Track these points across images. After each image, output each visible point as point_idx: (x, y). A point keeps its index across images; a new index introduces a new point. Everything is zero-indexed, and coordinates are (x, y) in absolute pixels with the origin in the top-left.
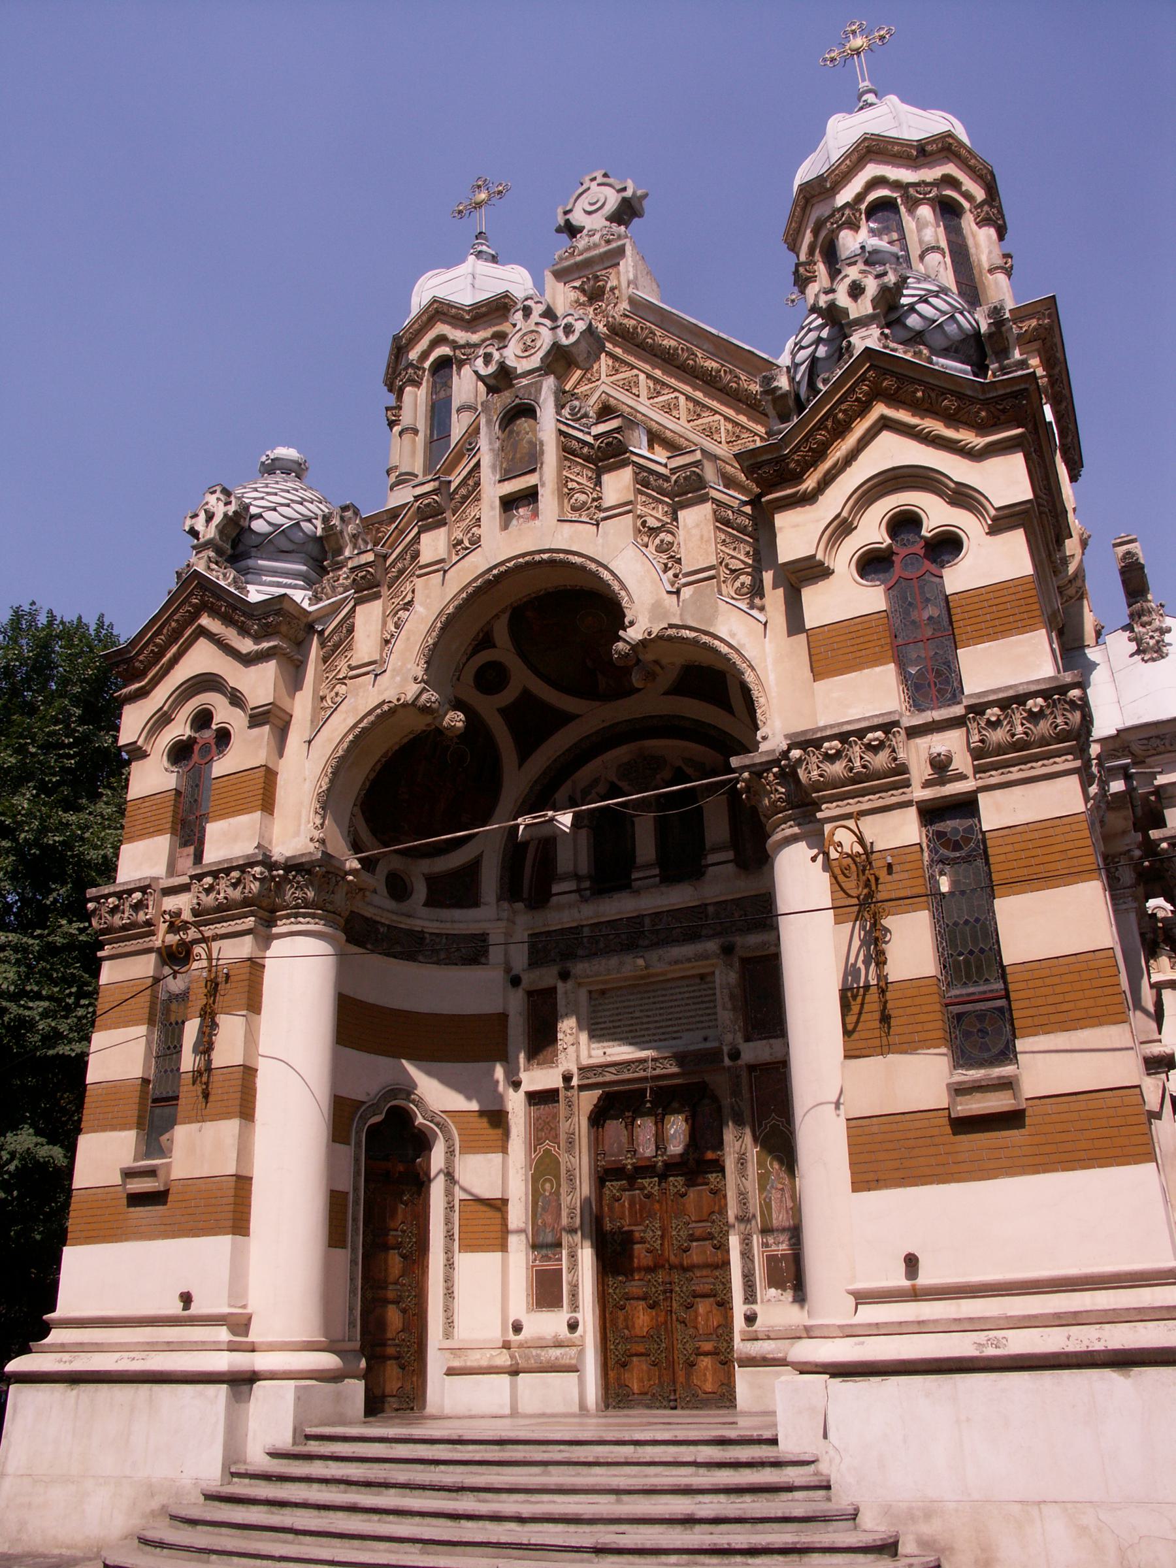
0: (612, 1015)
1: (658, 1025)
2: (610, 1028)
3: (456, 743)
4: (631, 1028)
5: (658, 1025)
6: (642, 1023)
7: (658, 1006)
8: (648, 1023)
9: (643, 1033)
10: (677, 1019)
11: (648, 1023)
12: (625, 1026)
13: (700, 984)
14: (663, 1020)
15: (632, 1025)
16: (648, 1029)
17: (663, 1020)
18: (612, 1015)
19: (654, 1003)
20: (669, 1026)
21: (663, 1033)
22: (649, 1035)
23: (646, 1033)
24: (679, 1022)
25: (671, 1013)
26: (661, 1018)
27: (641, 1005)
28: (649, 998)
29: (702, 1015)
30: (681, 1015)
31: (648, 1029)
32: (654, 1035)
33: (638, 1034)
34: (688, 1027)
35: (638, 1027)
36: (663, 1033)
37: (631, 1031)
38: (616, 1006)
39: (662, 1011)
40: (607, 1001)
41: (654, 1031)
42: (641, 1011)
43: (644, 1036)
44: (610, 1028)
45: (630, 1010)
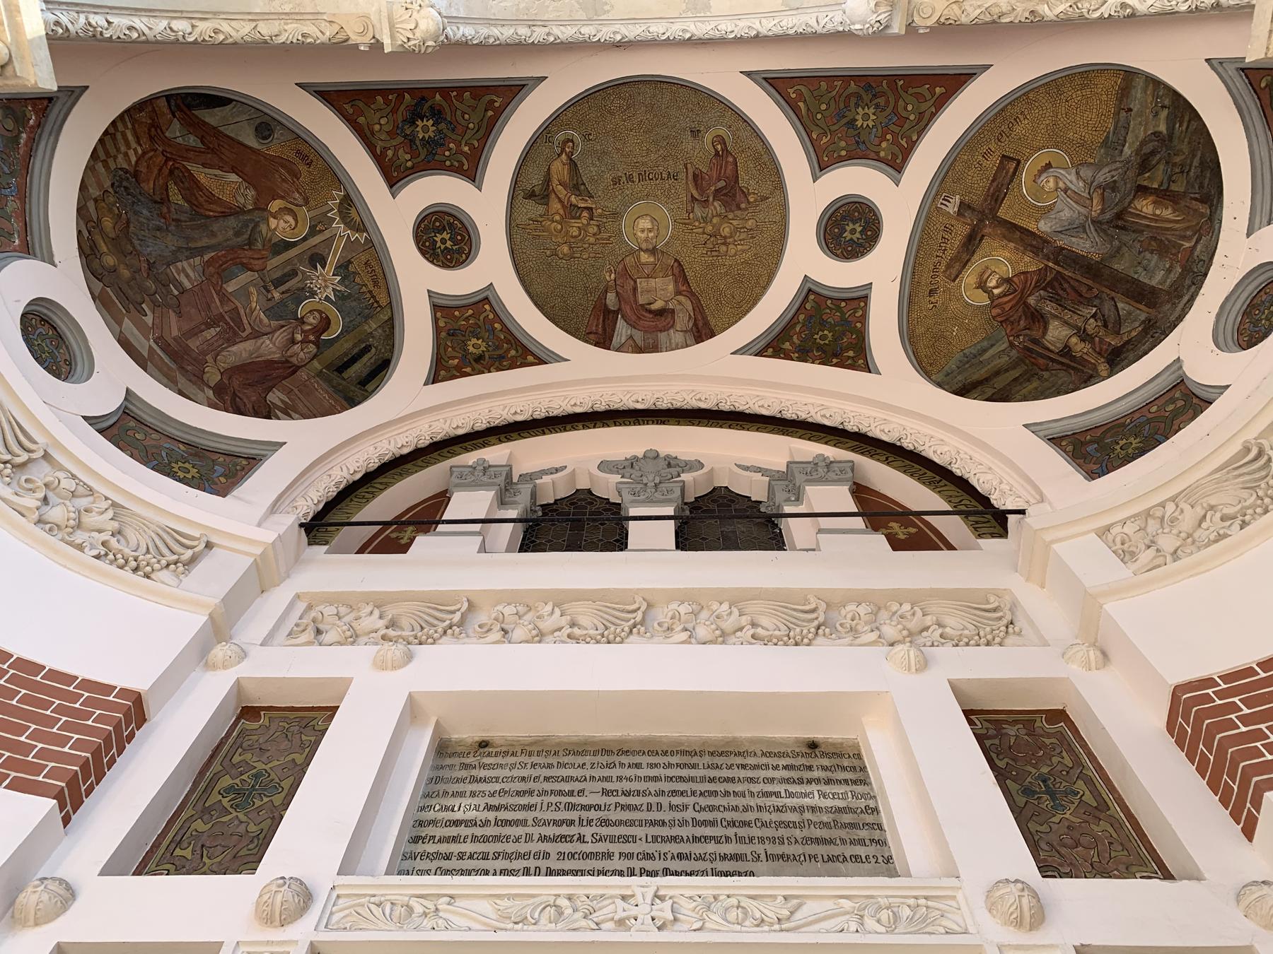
0: (503, 792)
1: (665, 831)
2: (486, 823)
3: (327, 298)
4: (564, 830)
5: (665, 831)
6: (605, 823)
7: (667, 787)
8: (631, 823)
9: (601, 847)
10: (732, 824)
11: (631, 823)
12: (537, 822)
13: (809, 755)
14: (683, 823)
15: (572, 823)
16: (626, 839)
17: (683, 823)
18: (503, 792)
19: (656, 779)
20: (706, 839)
21: (681, 856)
22: (629, 856)
23: (615, 848)
24: (742, 832)
25: (712, 808)
26: (678, 815)
27: (607, 779)
28: (638, 766)
29: (826, 825)
30: (750, 816)
31: (626, 839)
32: (649, 856)
33: (588, 848)
34: (778, 849)
35: (587, 831)
36: (681, 856)
37: (563, 838)
38: (524, 773)
39: (677, 800)
40: (487, 760)
41: (651, 848)
42: (606, 793)
43: (609, 856)
44: (486, 823)
45: (566, 787)
